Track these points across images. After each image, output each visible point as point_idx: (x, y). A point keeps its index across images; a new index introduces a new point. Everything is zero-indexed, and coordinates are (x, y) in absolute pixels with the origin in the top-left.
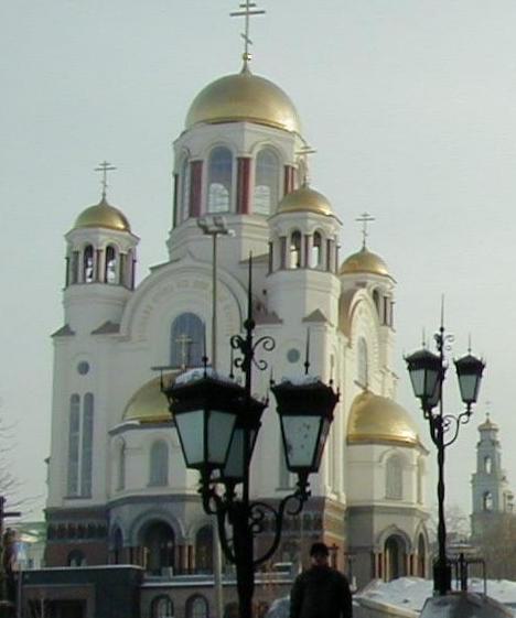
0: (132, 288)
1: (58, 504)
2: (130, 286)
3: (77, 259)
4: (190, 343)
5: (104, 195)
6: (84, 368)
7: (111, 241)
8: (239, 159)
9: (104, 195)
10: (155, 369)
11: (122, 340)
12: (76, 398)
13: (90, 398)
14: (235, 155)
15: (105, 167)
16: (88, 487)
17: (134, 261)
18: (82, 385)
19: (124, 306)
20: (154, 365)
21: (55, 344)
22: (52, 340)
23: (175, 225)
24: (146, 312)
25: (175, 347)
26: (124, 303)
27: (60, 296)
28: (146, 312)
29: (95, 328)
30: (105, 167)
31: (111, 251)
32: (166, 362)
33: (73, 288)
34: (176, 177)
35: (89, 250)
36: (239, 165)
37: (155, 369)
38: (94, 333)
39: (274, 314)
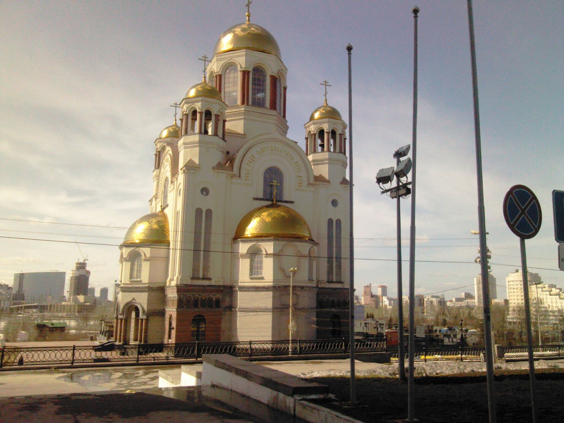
1: (185, 283)
11: (233, 176)
12: (199, 212)
13: (209, 212)
18: (205, 203)
20: (255, 197)
32: (261, 196)
38: (214, 168)
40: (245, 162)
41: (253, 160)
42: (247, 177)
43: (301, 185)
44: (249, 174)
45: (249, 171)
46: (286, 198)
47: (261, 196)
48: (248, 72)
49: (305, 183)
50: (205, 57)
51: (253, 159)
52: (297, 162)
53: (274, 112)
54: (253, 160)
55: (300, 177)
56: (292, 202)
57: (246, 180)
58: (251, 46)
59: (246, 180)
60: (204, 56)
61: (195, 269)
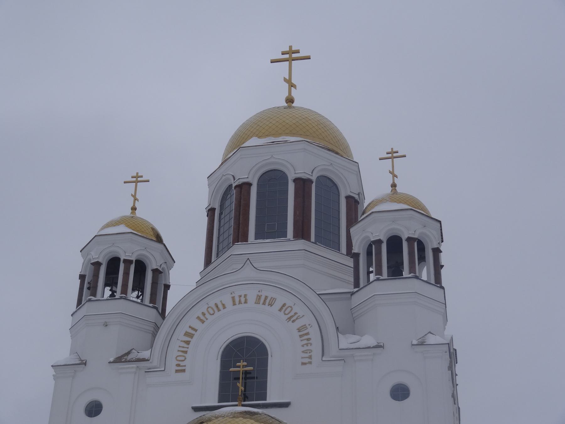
0: (163, 314)
3: (96, 275)
7: (144, 252)
8: (296, 180)
10: (196, 409)
14: (291, 176)
17: (167, 287)
19: (154, 335)
21: (55, 377)
22: (52, 372)
23: (208, 261)
24: (187, 334)
26: (157, 328)
27: (68, 321)
28: (187, 334)
29: (112, 359)
30: (137, 179)
31: (141, 266)
33: (87, 308)
34: (211, 212)
35: (114, 263)
46: (270, 399)
50: (137, 176)
53: (301, 244)
56: (286, 405)
60: (135, 175)
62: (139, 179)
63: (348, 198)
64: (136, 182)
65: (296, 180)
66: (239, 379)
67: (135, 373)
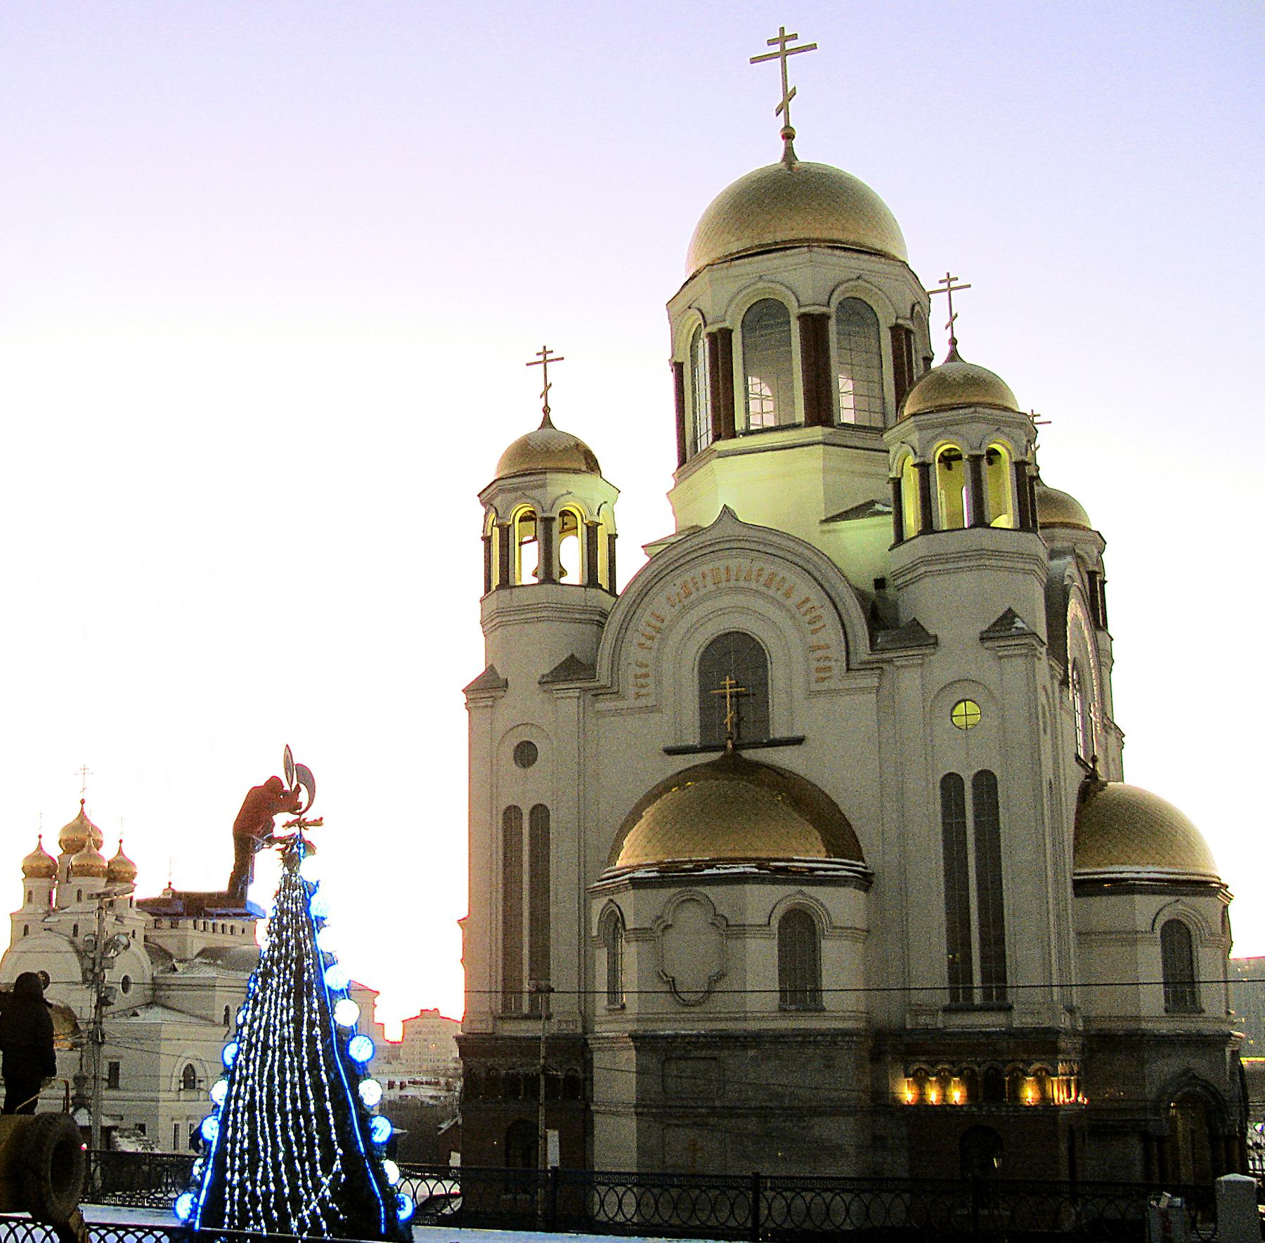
0: (612, 590)
2: (606, 586)
4: (738, 695)
5: (546, 410)
6: (526, 754)
9: (546, 410)
10: (670, 752)
11: (598, 693)
13: (540, 813)
15: (545, 357)
16: (543, 991)
17: (612, 538)
19: (601, 625)
20: (671, 744)
25: (709, 705)
30: (545, 357)
36: (803, 330)
37: (670, 752)
39: (915, 624)
40: (634, 637)
41: (659, 630)
42: (642, 686)
43: (823, 675)
44: (646, 676)
45: (646, 666)
46: (778, 732)
47: (693, 739)
48: (727, 334)
49: (839, 667)
50: (545, 352)
51: (658, 624)
52: (807, 600)
54: (659, 630)
55: (819, 648)
56: (799, 741)
57: (638, 696)
58: (734, 248)
59: (638, 696)
61: (510, 989)
62: (549, 357)
63: (896, 330)
64: (545, 362)
65: (803, 318)
66: (726, 697)
67: (579, 698)
